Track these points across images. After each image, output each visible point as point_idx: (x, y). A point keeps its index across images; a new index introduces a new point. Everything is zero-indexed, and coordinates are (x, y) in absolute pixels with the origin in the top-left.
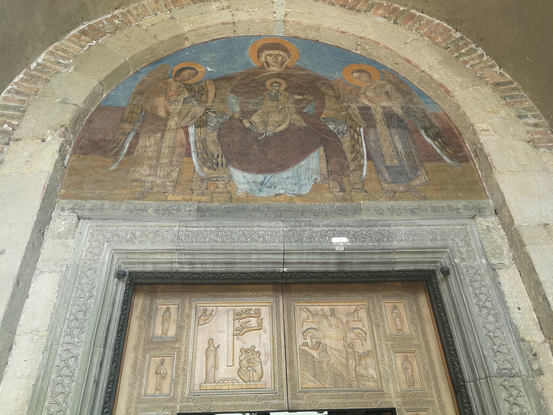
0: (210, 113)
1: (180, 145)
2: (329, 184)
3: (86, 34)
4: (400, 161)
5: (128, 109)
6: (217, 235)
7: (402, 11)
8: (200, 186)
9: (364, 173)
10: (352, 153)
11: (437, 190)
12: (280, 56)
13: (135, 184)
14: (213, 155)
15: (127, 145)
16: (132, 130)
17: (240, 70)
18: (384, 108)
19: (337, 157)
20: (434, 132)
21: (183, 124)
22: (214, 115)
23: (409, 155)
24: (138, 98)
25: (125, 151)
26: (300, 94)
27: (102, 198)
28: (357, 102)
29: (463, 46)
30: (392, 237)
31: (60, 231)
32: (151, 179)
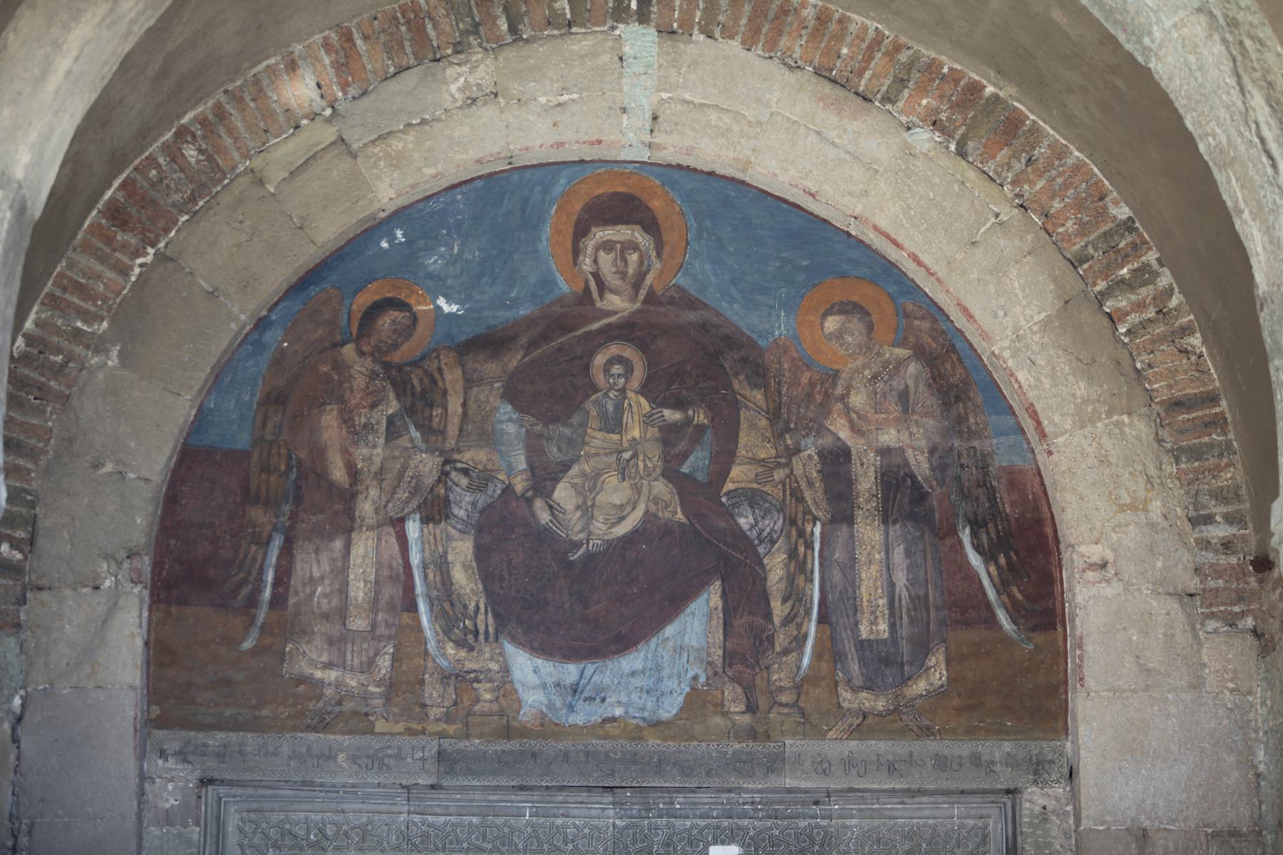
0: (453, 475)
1: (391, 577)
2: (723, 692)
3: (126, 223)
4: (892, 626)
5: (255, 456)
6: (484, 837)
7: (988, 99)
8: (441, 696)
9: (806, 661)
10: (785, 601)
11: (959, 710)
12: (635, 247)
13: (301, 688)
14: (465, 607)
15: (270, 576)
16: (275, 529)
17: (524, 311)
18: (885, 452)
19: (750, 613)
20: (993, 535)
21: (393, 510)
22: (464, 481)
23: (919, 602)
24: (275, 419)
25: (267, 594)
26: (679, 405)
27: (237, 727)
28: (821, 430)
29: (1127, 256)
30: (829, 844)
31: (168, 806)
32: (333, 675)
